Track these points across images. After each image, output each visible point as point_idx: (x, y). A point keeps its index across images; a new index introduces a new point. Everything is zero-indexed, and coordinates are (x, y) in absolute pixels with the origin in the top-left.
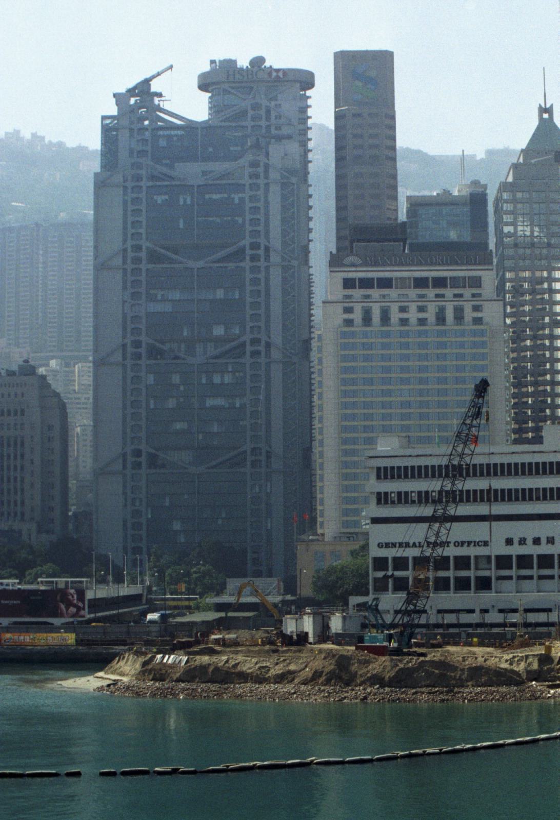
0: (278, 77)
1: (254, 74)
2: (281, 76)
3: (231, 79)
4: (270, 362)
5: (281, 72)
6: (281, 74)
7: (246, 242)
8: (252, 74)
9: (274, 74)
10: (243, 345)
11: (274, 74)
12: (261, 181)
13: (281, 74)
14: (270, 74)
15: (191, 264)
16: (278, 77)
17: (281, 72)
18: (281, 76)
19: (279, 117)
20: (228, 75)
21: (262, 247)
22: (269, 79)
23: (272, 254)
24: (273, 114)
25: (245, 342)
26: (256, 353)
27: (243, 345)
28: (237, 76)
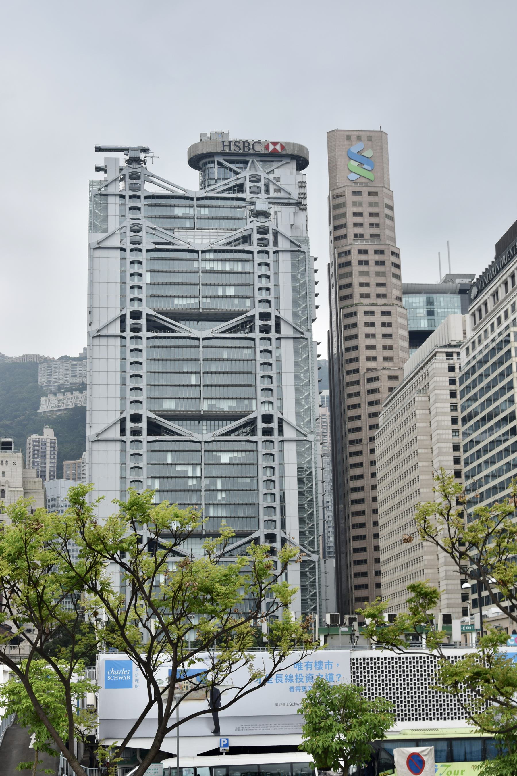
0: (275, 150)
1: (251, 146)
2: (280, 150)
3: (227, 150)
4: (283, 441)
5: (279, 145)
6: (278, 147)
7: (256, 311)
8: (248, 146)
9: (271, 147)
10: (254, 421)
11: (271, 147)
12: (271, 248)
13: (278, 147)
14: (267, 147)
15: (195, 333)
16: (275, 150)
17: (279, 145)
18: (280, 150)
19: (279, 190)
20: (224, 146)
21: (273, 317)
22: (266, 152)
23: (283, 325)
24: (272, 188)
25: (256, 418)
26: (267, 432)
27: (254, 421)
28: (233, 147)
